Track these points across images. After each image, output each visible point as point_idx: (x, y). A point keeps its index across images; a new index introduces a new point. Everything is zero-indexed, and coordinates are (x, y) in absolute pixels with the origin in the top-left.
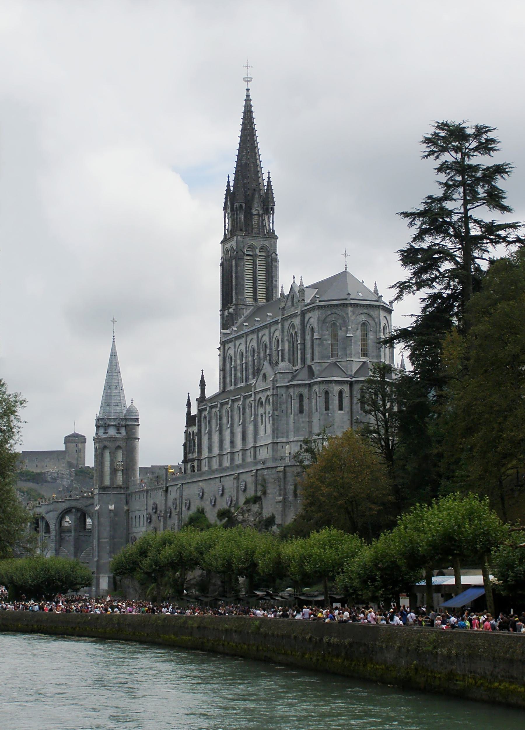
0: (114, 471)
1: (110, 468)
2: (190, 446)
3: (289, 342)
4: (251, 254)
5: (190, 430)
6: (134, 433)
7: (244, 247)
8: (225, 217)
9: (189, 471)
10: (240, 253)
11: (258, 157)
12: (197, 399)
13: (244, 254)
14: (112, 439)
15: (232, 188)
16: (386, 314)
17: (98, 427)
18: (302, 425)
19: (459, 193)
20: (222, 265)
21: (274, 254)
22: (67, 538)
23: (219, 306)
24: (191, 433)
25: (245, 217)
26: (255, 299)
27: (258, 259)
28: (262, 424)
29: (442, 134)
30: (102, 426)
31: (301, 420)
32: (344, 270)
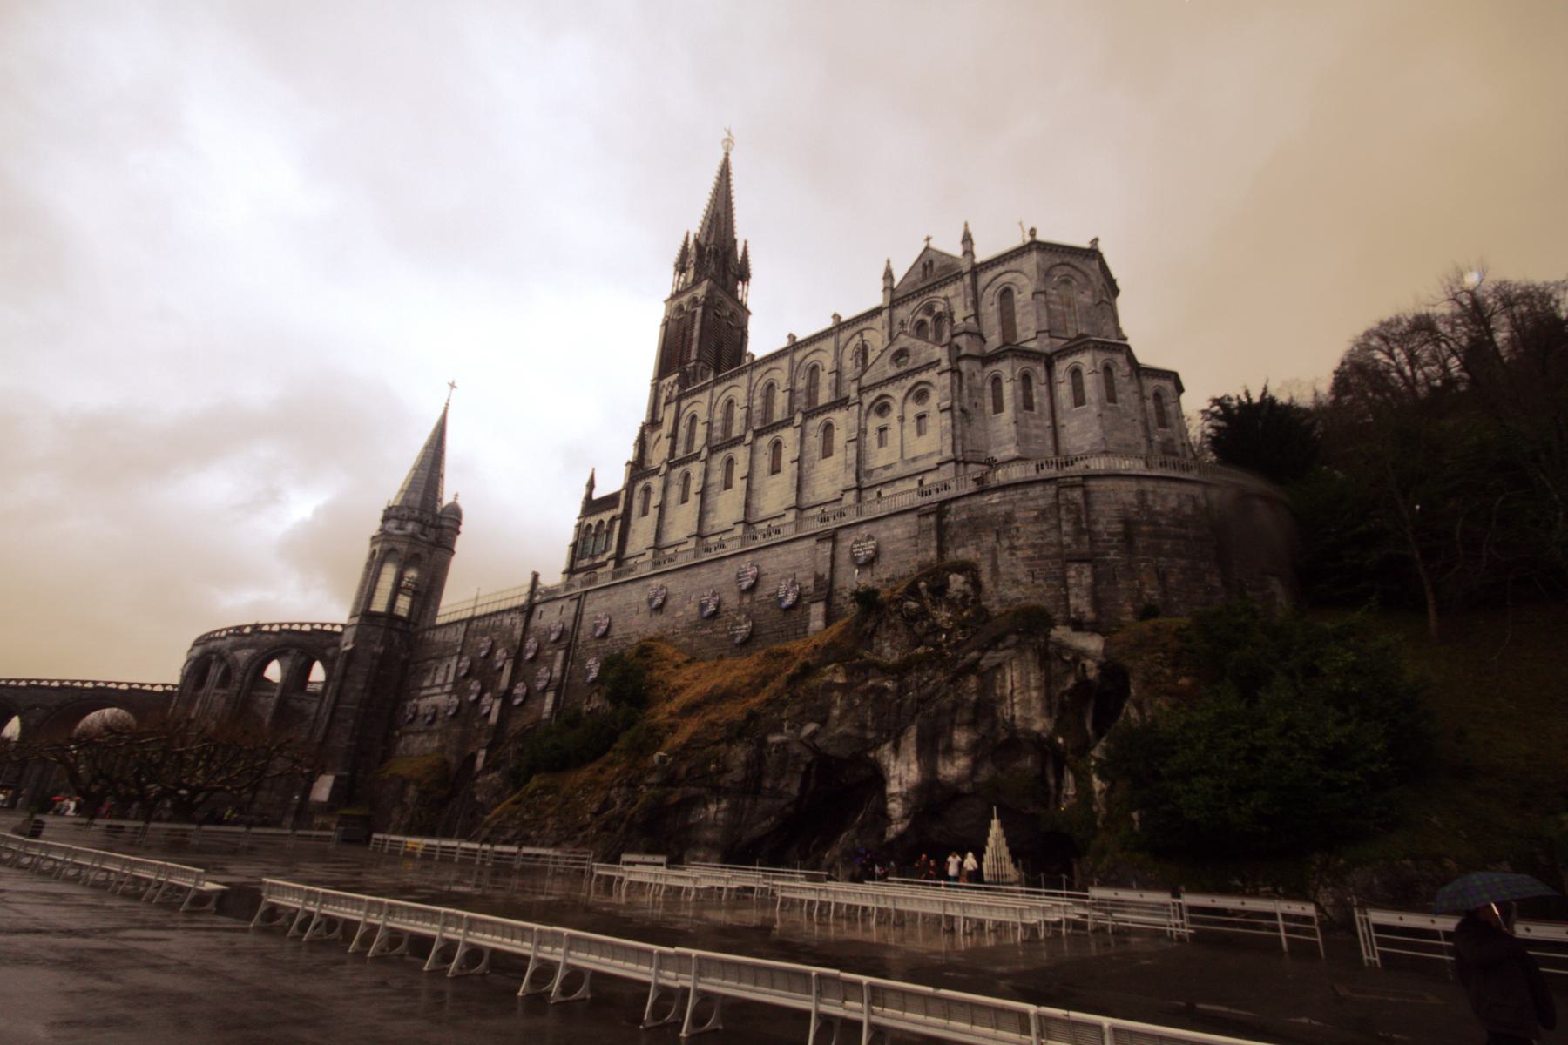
0: (397, 589)
5: (593, 520)
6: (453, 541)
12: (629, 463)
17: (386, 519)
18: (1035, 431)
22: (262, 700)
31: (1031, 422)
32: (1028, 239)
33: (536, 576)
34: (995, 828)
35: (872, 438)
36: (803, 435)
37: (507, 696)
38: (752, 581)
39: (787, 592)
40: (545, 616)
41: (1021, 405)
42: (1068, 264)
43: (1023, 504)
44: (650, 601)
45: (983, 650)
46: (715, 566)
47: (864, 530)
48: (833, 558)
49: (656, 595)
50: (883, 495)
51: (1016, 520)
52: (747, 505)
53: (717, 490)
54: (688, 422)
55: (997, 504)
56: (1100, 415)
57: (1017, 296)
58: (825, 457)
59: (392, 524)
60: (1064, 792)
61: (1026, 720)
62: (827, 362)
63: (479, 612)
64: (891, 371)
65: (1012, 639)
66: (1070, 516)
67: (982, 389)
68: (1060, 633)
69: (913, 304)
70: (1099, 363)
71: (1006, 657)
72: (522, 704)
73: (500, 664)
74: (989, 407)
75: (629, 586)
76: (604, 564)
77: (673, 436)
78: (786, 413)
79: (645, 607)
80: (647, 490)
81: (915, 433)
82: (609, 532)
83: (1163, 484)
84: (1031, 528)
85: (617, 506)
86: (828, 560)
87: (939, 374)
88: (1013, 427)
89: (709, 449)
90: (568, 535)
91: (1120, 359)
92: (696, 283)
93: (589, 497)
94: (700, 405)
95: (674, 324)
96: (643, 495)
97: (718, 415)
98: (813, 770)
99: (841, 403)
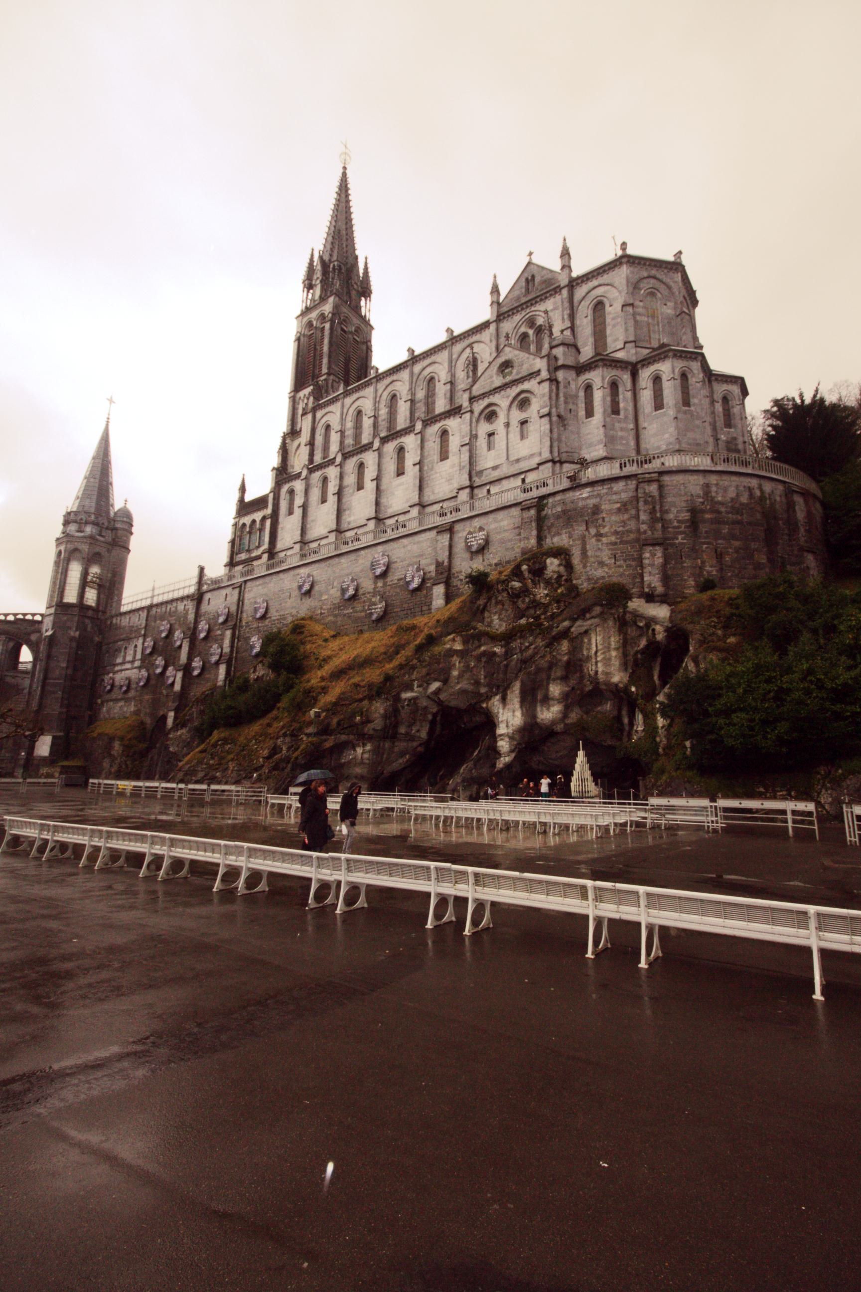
5: (247, 520)
6: (128, 541)
12: (274, 469)
17: (66, 523)
18: (620, 434)
20: (298, 340)
31: (617, 425)
32: (620, 253)
33: (202, 569)
34: (581, 757)
35: (482, 442)
36: (423, 441)
37: (187, 669)
38: (384, 568)
39: (413, 577)
40: (212, 602)
41: (609, 410)
42: (654, 277)
43: (609, 497)
44: (300, 587)
45: (574, 620)
46: (352, 557)
47: (477, 523)
48: (451, 547)
49: (304, 582)
50: (492, 493)
51: (602, 512)
52: (377, 504)
53: (351, 491)
54: (323, 431)
55: (587, 498)
56: (676, 418)
57: (608, 309)
58: (441, 460)
59: (72, 528)
60: (635, 728)
61: (607, 674)
62: (443, 374)
63: (156, 600)
64: (498, 381)
65: (597, 610)
66: (647, 507)
67: (577, 396)
68: (636, 604)
69: (517, 318)
70: (677, 370)
71: (592, 625)
72: (200, 675)
73: (178, 643)
74: (582, 413)
75: (281, 575)
76: (259, 557)
77: (311, 444)
78: (408, 421)
79: (296, 593)
80: (291, 492)
81: (519, 437)
82: (261, 530)
83: (725, 477)
84: (614, 518)
85: (266, 507)
86: (447, 549)
87: (539, 383)
88: (602, 430)
89: (343, 455)
90: (228, 534)
91: (695, 366)
92: (323, 299)
93: (241, 500)
94: (333, 415)
95: (306, 339)
96: (288, 496)
97: (349, 424)
98: (438, 718)
99: (455, 411)
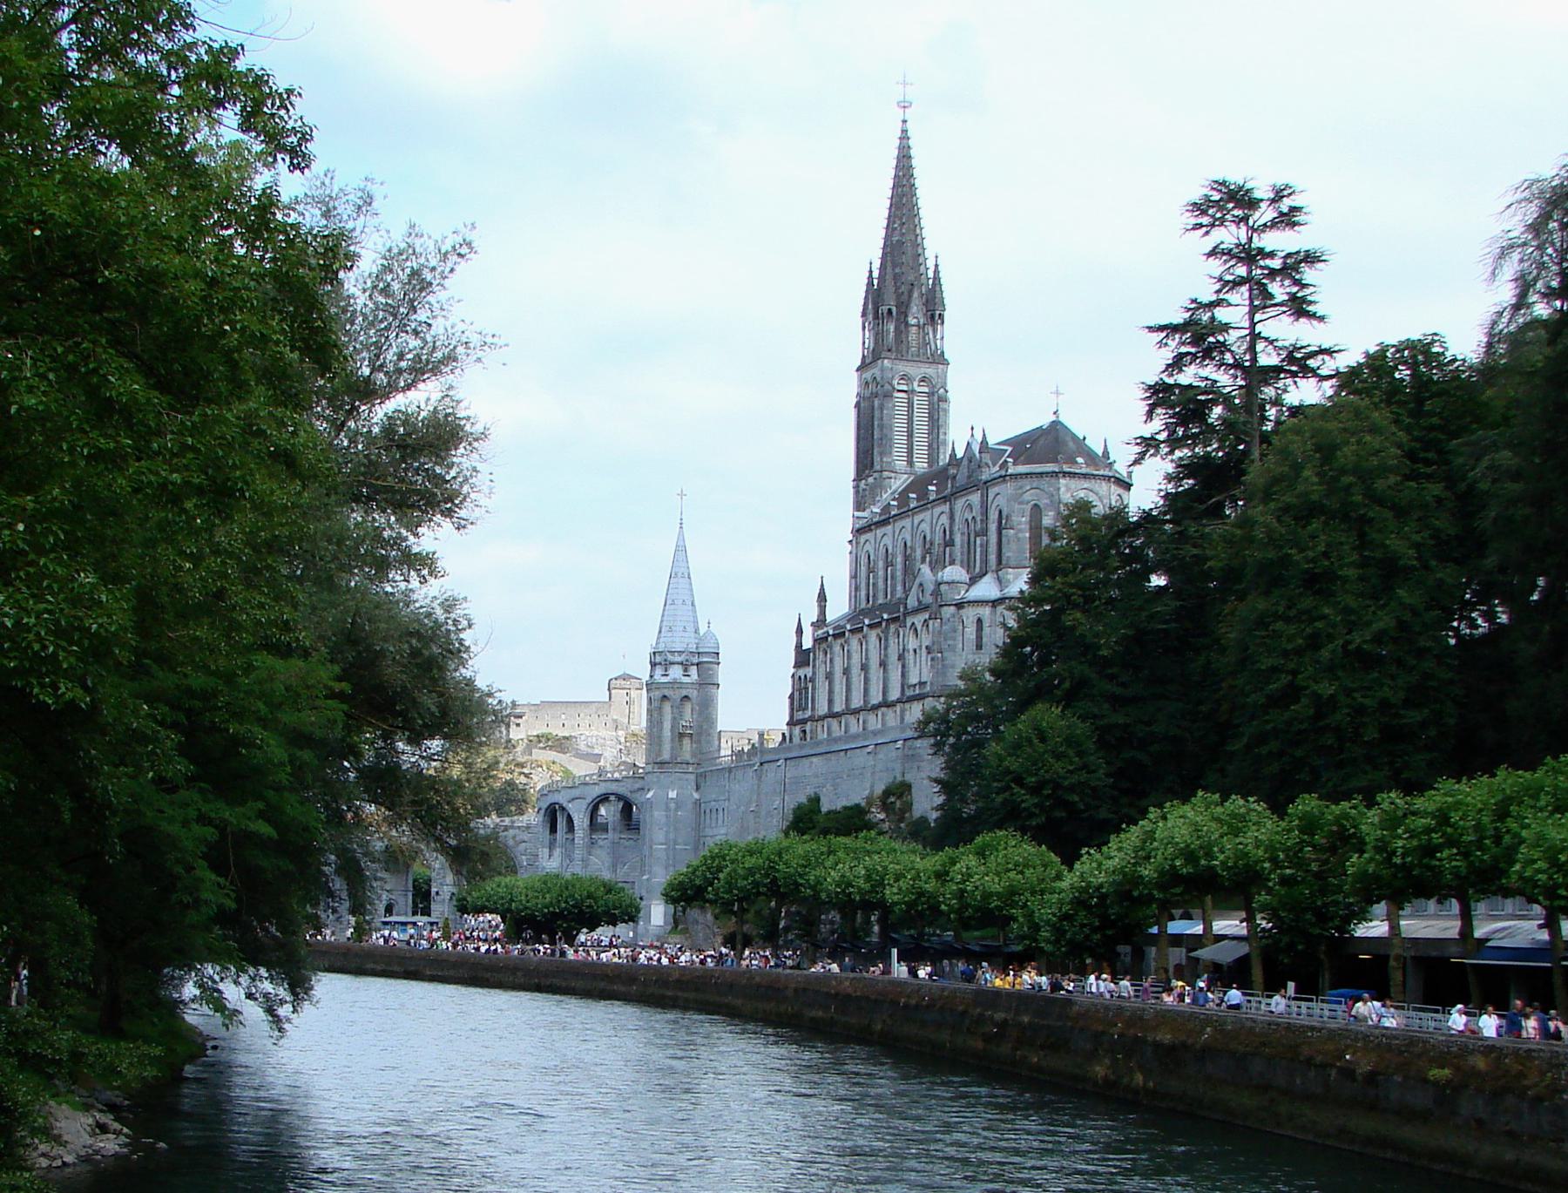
1: (672, 731)
2: (800, 699)
3: (963, 534)
4: (905, 388)
5: (801, 672)
6: (711, 676)
7: (893, 378)
8: (864, 328)
9: (796, 740)
10: (887, 387)
11: (918, 231)
13: (894, 388)
14: (675, 684)
15: (875, 282)
16: (1120, 491)
17: (653, 665)
19: (1240, 296)
20: (857, 405)
21: (942, 390)
22: (601, 843)
23: (851, 473)
24: (803, 677)
25: (898, 331)
26: (910, 463)
27: (916, 398)
28: (915, 665)
29: (1216, 197)
30: (660, 664)
32: (1053, 418)
